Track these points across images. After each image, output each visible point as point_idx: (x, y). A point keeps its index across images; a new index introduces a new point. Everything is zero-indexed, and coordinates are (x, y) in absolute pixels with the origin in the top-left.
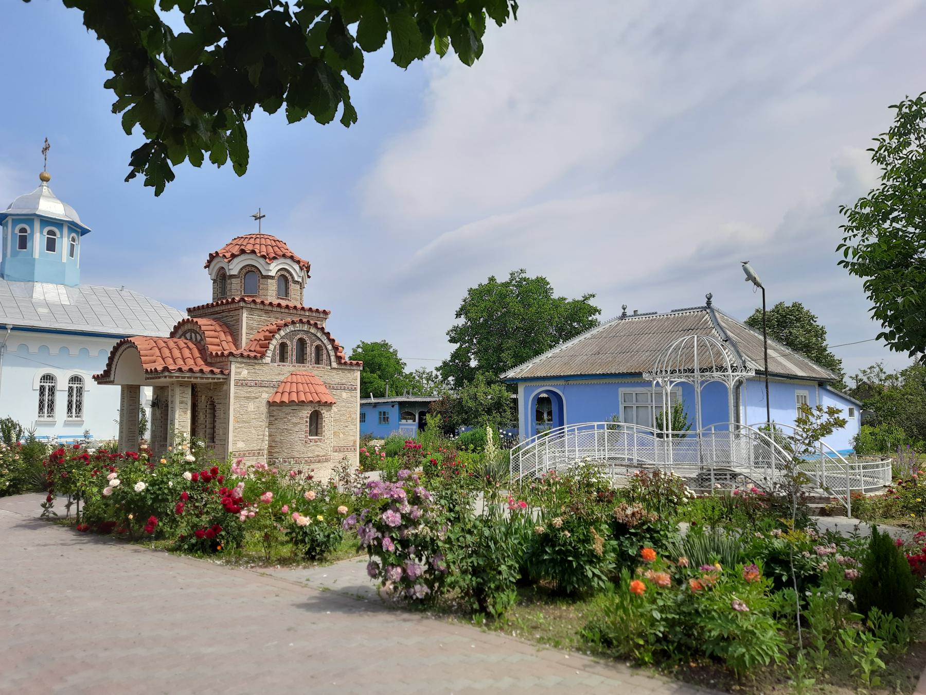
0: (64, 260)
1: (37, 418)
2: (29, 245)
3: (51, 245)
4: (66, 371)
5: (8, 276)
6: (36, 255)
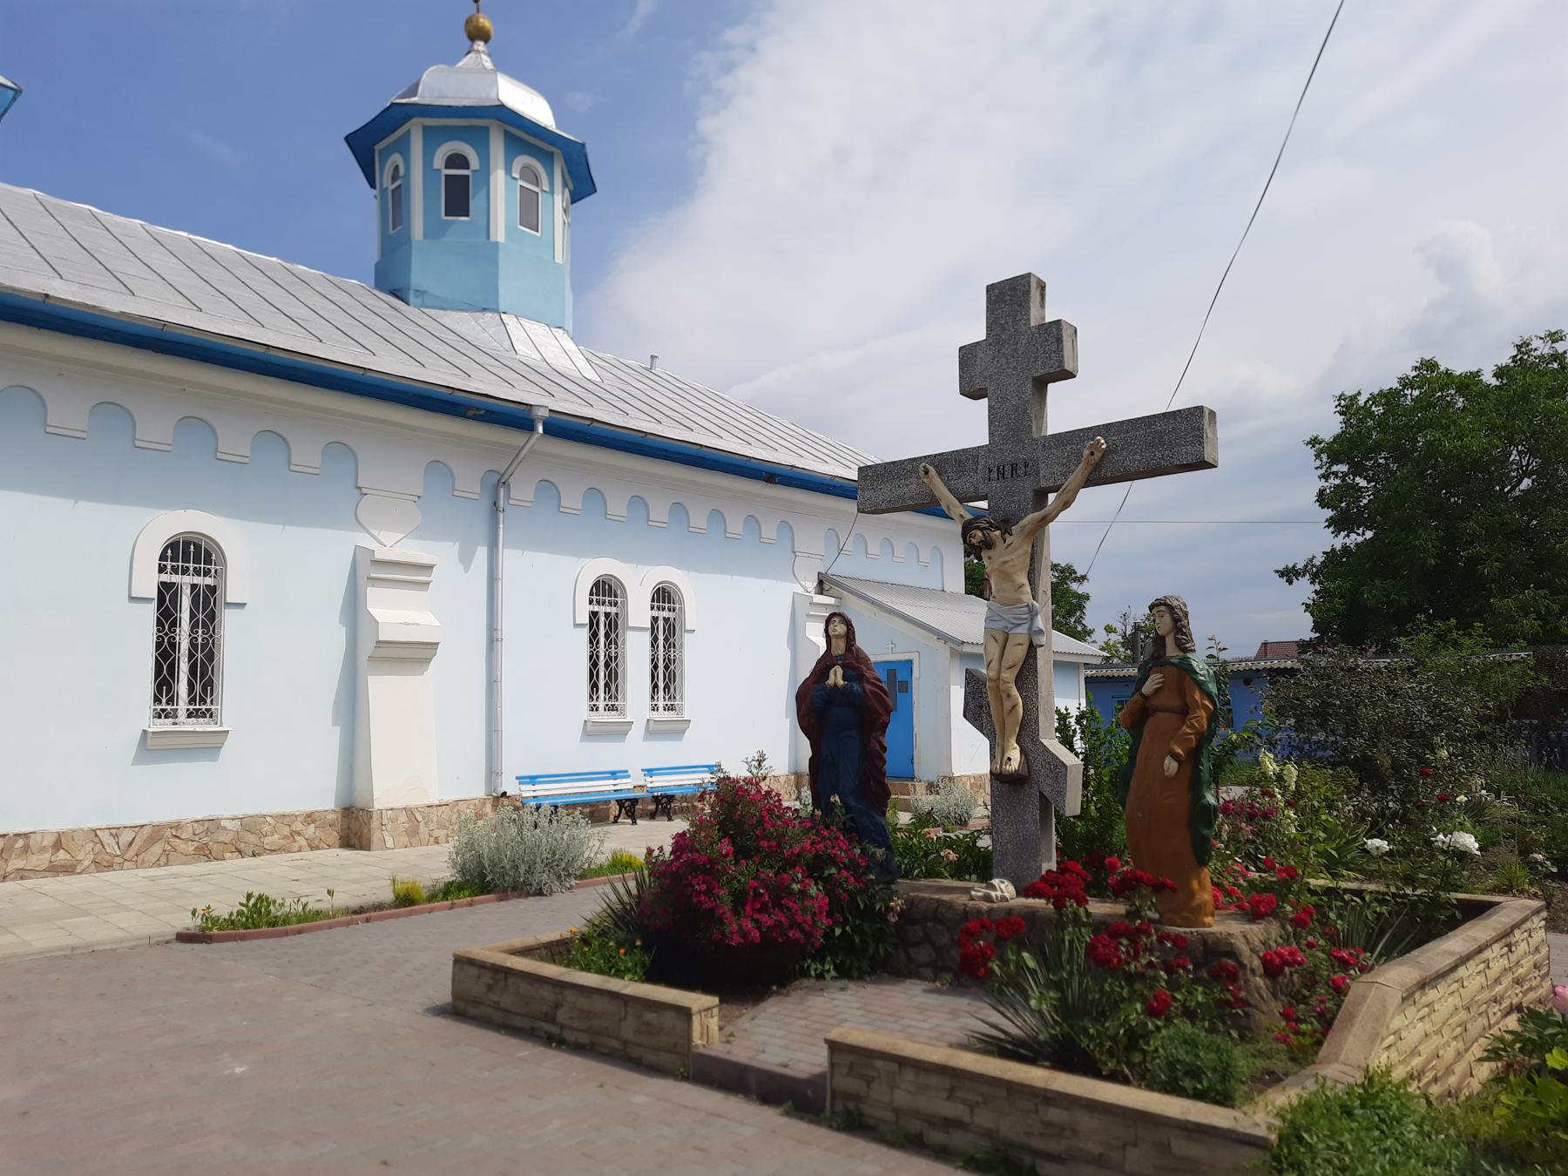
0: (559, 259)
1: (585, 714)
2: (475, 203)
3: (529, 214)
4: (643, 569)
5: (420, 293)
6: (499, 234)
